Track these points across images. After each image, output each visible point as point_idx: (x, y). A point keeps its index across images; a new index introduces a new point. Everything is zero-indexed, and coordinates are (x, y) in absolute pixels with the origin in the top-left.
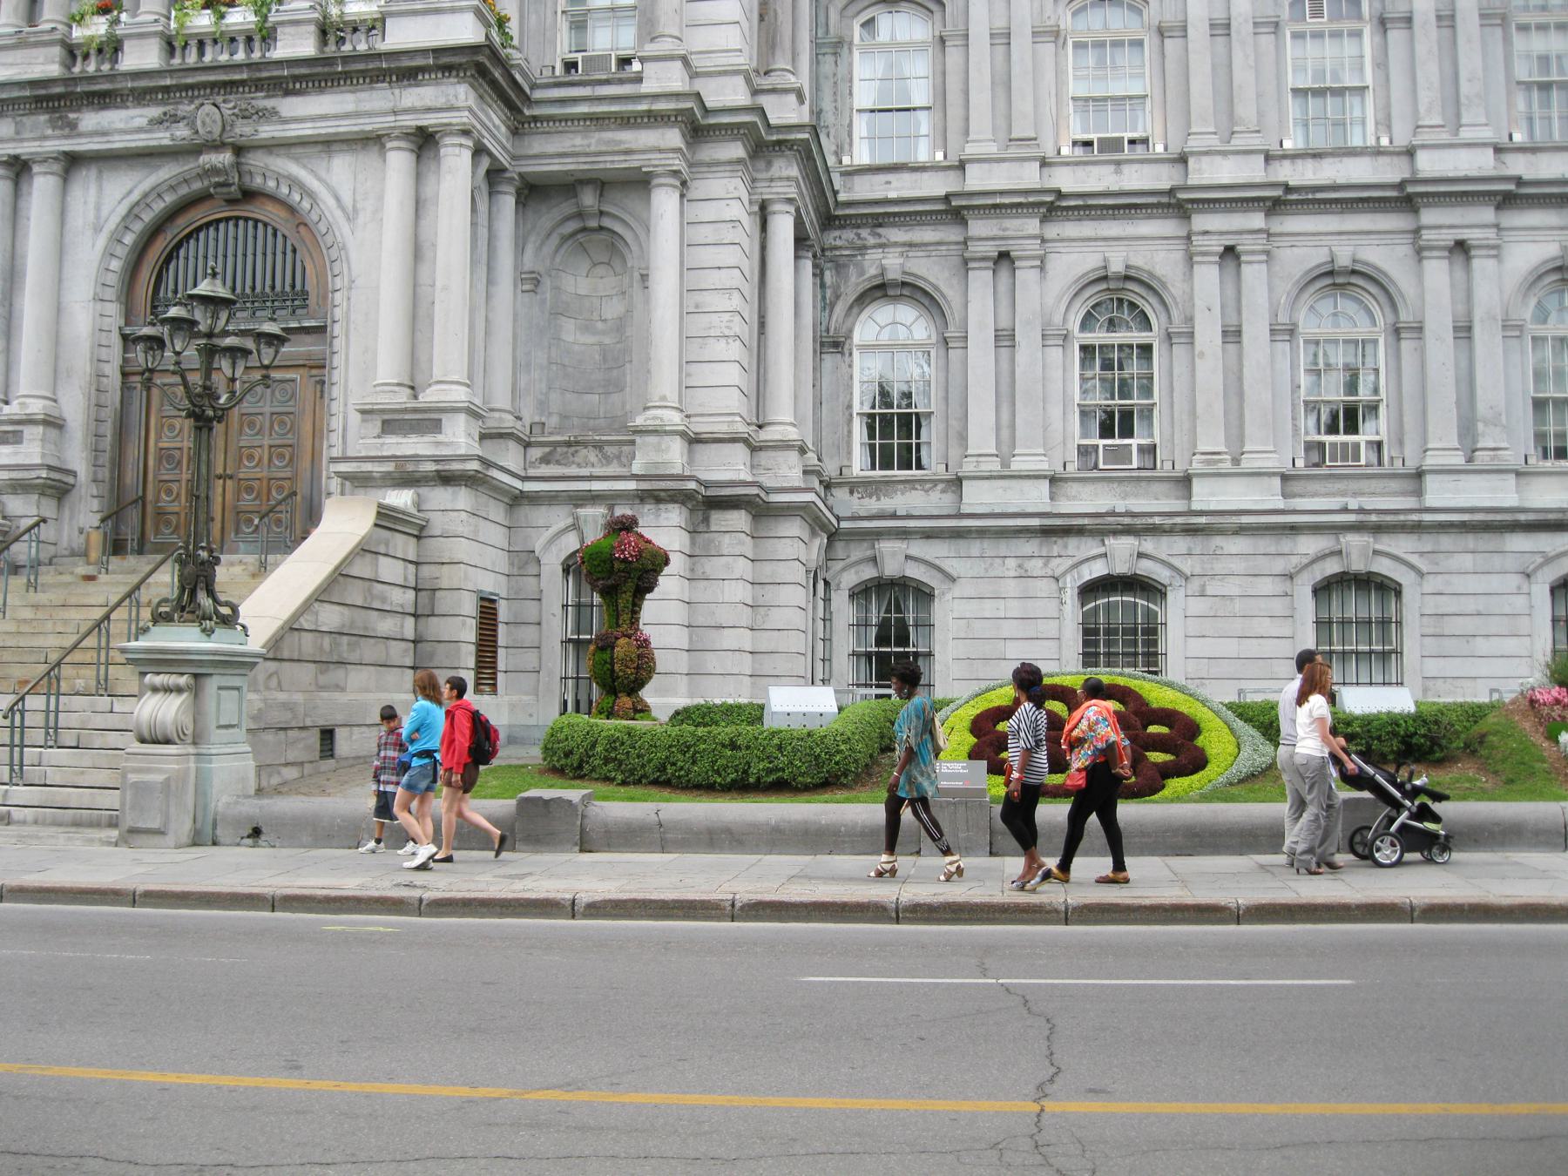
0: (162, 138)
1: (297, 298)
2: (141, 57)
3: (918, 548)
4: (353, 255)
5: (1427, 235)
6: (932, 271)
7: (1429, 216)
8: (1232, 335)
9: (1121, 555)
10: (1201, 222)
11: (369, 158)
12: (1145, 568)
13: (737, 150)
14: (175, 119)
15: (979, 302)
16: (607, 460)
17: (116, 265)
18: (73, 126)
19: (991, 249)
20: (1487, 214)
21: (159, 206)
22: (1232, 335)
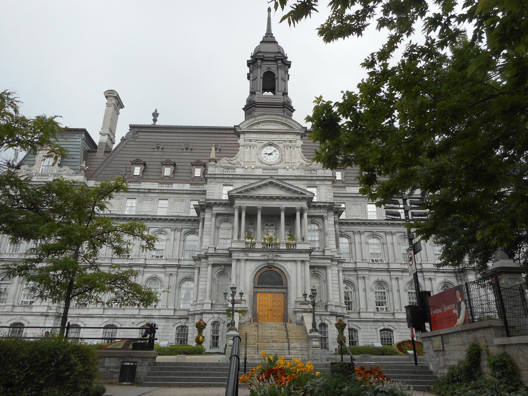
0: (263, 258)
1: (281, 283)
2: (259, 246)
3: (354, 323)
4: (292, 277)
5: (425, 277)
6: (353, 279)
7: (425, 274)
8: (398, 291)
9: (386, 325)
10: (392, 273)
11: (293, 264)
12: (390, 327)
13: (336, 263)
15: (361, 284)
16: (321, 309)
17: (253, 276)
18: (248, 255)
19: (361, 276)
20: (433, 274)
21: (260, 268)
22: (398, 291)
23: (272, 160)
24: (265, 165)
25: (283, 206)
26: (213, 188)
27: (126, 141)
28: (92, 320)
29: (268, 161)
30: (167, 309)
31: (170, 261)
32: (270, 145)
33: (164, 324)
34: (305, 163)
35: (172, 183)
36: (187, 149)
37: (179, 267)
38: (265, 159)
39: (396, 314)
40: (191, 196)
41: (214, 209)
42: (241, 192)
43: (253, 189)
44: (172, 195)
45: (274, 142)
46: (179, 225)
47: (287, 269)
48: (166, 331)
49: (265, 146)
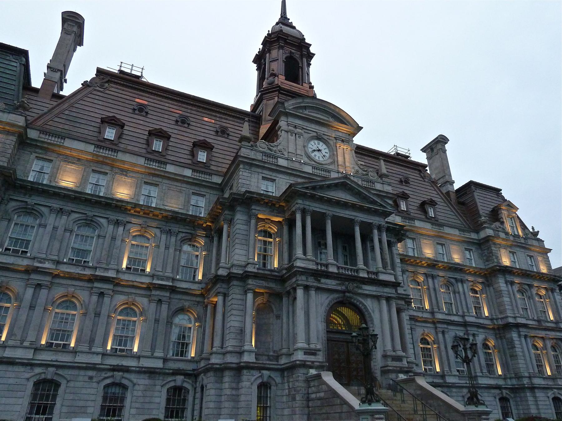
0: (339, 288)
4: (375, 320)
5: (469, 332)
14: (343, 285)
18: (319, 281)
23: (321, 159)
24: (313, 163)
26: (249, 178)
27: (90, 89)
28: (10, 368)
29: (317, 158)
30: (152, 357)
31: (158, 279)
32: (319, 138)
33: (147, 382)
34: (360, 171)
35: (165, 163)
36: (183, 122)
37: (173, 290)
38: (313, 155)
39: (447, 377)
40: (193, 187)
41: (253, 207)
43: (322, 187)
44: (165, 181)
45: (323, 136)
46: (175, 228)
47: (368, 307)
48: (148, 393)
49: (313, 138)
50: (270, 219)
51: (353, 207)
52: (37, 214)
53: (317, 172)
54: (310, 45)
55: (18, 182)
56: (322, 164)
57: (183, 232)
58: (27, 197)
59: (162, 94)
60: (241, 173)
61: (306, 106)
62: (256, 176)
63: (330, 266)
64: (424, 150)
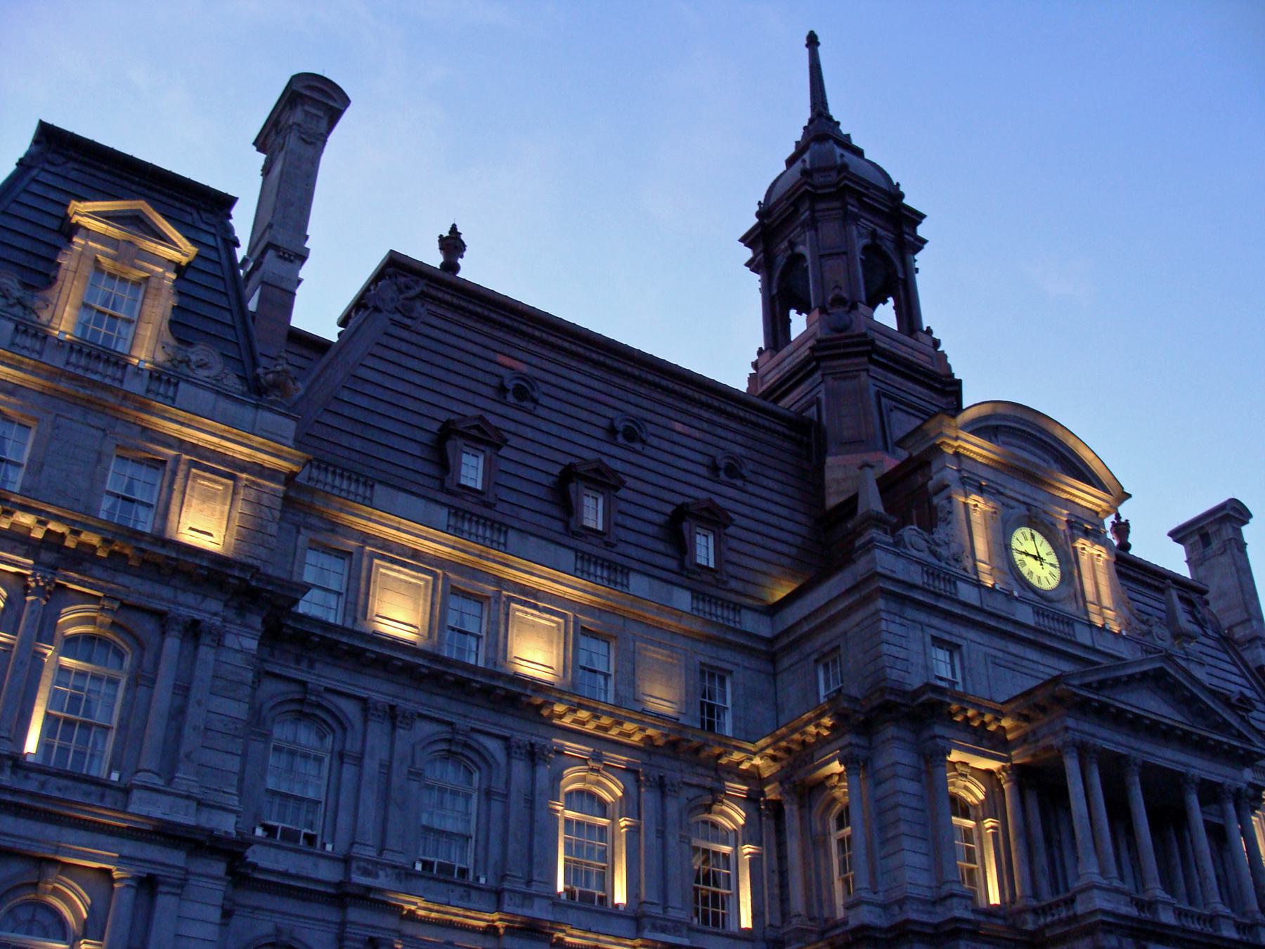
24: (1031, 595)
25: (1196, 772)
36: (630, 435)
42: (1088, 686)
50: (966, 764)
51: (1185, 740)
52: (329, 720)
53: (1047, 624)
54: (922, 216)
55: (290, 623)
56: (1050, 601)
57: (691, 785)
58: (304, 666)
59: (559, 342)
60: (883, 625)
61: (997, 427)
62: (919, 633)
63: (1160, 907)
64: (1179, 535)
